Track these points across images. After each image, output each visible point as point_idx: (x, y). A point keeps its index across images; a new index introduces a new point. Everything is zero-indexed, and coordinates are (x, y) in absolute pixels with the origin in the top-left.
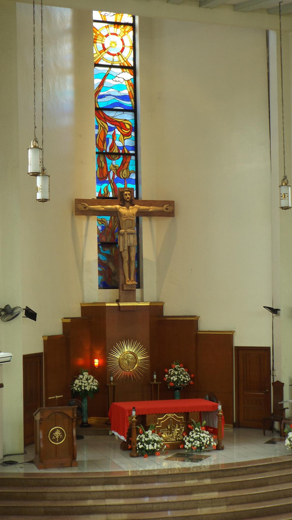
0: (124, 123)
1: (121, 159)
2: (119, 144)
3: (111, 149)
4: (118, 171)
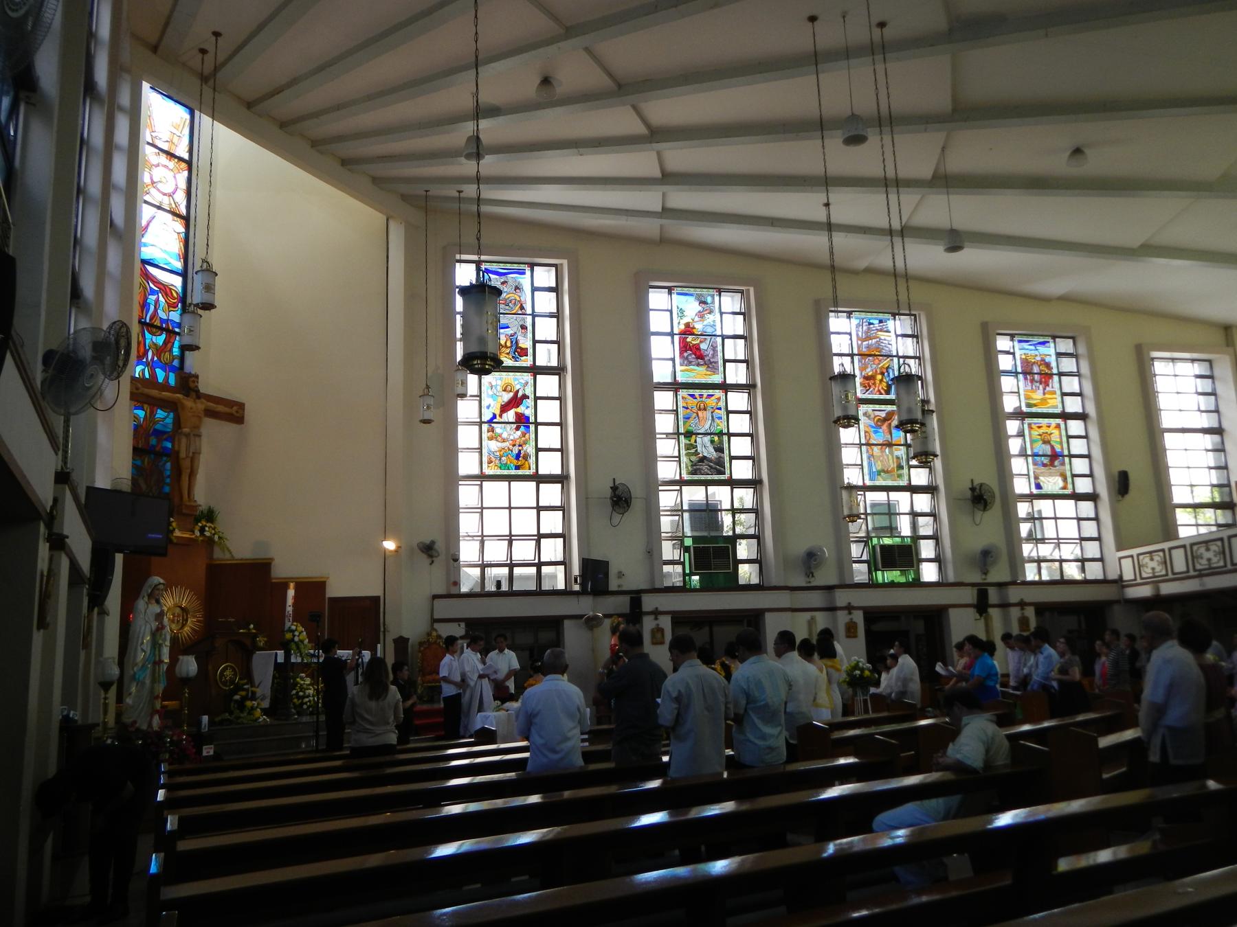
1: (164, 336)
2: (162, 315)
3: (151, 319)
4: (159, 351)
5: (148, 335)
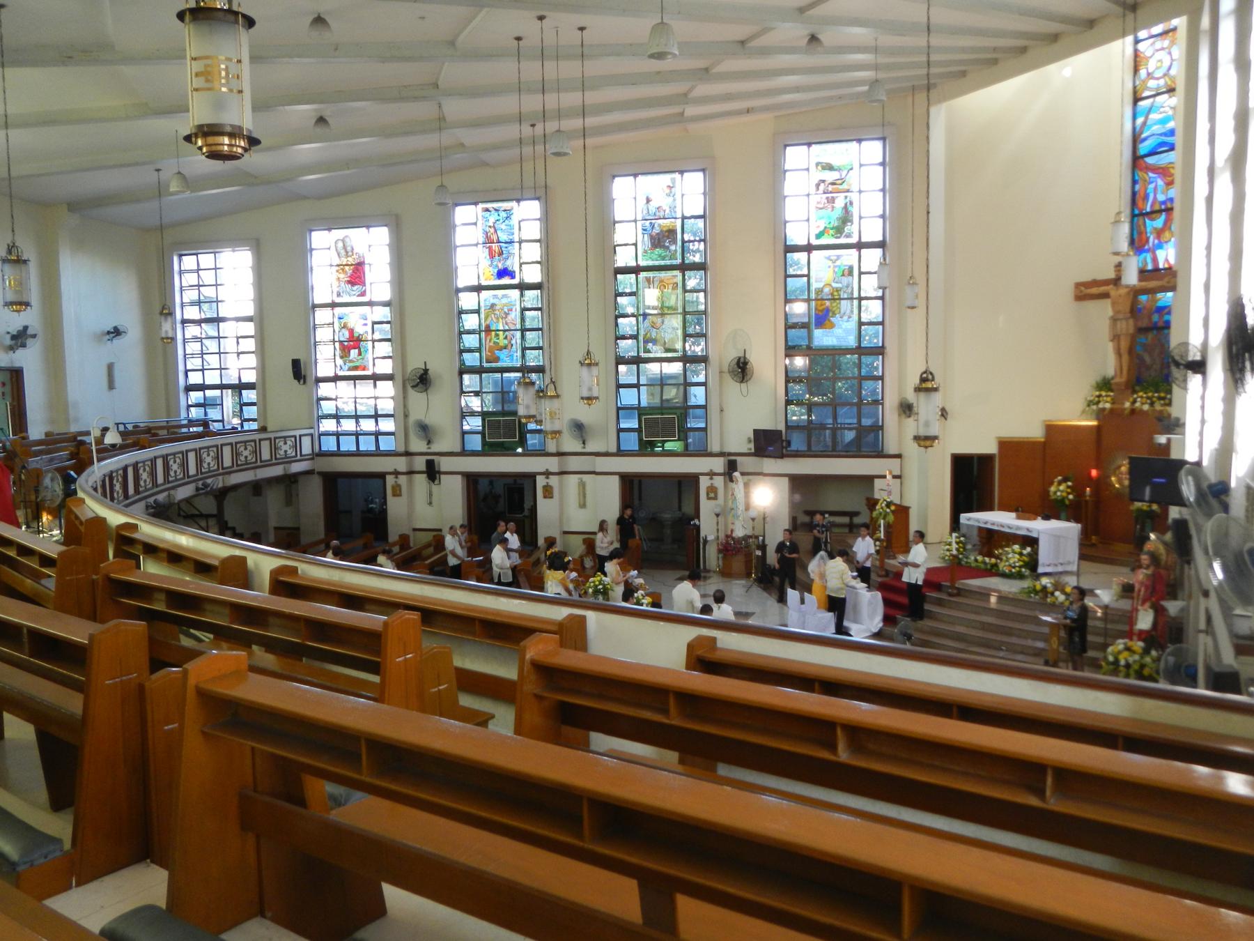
2: (1161, 197)
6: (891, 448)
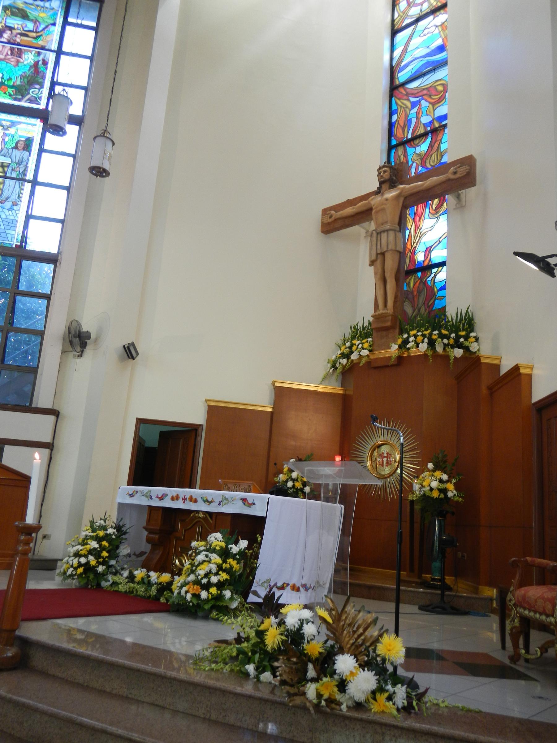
0: (435, 86)
2: (425, 119)
3: (413, 132)
4: (423, 159)
5: (410, 151)
6: (43, 399)
